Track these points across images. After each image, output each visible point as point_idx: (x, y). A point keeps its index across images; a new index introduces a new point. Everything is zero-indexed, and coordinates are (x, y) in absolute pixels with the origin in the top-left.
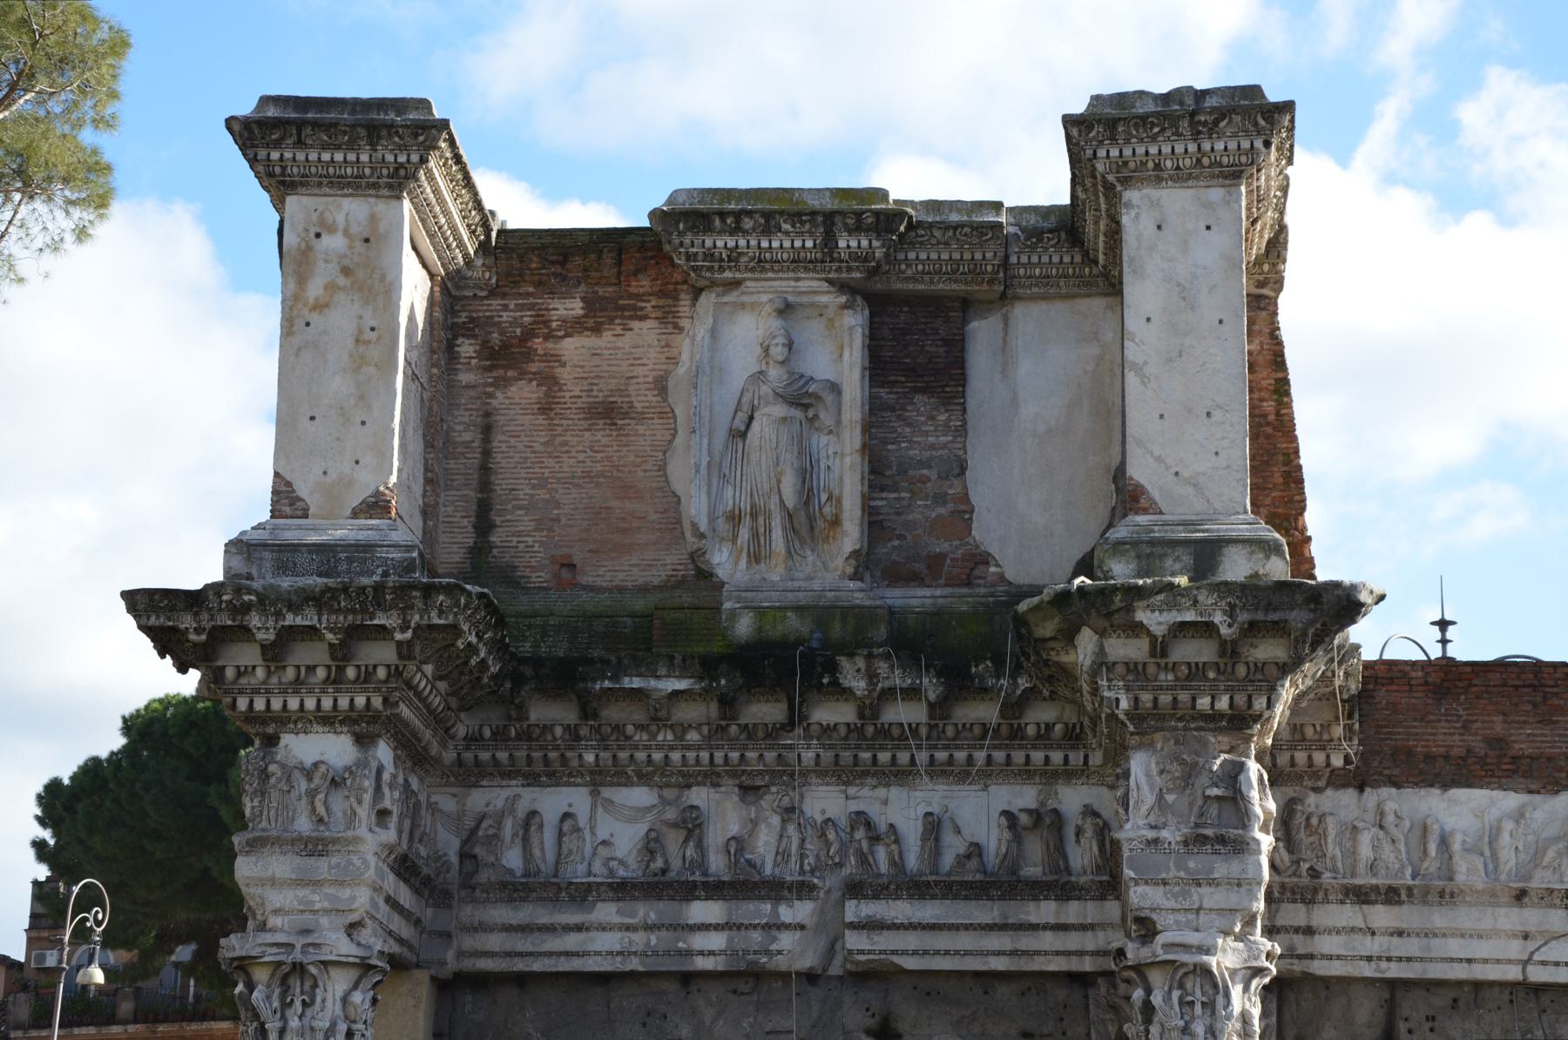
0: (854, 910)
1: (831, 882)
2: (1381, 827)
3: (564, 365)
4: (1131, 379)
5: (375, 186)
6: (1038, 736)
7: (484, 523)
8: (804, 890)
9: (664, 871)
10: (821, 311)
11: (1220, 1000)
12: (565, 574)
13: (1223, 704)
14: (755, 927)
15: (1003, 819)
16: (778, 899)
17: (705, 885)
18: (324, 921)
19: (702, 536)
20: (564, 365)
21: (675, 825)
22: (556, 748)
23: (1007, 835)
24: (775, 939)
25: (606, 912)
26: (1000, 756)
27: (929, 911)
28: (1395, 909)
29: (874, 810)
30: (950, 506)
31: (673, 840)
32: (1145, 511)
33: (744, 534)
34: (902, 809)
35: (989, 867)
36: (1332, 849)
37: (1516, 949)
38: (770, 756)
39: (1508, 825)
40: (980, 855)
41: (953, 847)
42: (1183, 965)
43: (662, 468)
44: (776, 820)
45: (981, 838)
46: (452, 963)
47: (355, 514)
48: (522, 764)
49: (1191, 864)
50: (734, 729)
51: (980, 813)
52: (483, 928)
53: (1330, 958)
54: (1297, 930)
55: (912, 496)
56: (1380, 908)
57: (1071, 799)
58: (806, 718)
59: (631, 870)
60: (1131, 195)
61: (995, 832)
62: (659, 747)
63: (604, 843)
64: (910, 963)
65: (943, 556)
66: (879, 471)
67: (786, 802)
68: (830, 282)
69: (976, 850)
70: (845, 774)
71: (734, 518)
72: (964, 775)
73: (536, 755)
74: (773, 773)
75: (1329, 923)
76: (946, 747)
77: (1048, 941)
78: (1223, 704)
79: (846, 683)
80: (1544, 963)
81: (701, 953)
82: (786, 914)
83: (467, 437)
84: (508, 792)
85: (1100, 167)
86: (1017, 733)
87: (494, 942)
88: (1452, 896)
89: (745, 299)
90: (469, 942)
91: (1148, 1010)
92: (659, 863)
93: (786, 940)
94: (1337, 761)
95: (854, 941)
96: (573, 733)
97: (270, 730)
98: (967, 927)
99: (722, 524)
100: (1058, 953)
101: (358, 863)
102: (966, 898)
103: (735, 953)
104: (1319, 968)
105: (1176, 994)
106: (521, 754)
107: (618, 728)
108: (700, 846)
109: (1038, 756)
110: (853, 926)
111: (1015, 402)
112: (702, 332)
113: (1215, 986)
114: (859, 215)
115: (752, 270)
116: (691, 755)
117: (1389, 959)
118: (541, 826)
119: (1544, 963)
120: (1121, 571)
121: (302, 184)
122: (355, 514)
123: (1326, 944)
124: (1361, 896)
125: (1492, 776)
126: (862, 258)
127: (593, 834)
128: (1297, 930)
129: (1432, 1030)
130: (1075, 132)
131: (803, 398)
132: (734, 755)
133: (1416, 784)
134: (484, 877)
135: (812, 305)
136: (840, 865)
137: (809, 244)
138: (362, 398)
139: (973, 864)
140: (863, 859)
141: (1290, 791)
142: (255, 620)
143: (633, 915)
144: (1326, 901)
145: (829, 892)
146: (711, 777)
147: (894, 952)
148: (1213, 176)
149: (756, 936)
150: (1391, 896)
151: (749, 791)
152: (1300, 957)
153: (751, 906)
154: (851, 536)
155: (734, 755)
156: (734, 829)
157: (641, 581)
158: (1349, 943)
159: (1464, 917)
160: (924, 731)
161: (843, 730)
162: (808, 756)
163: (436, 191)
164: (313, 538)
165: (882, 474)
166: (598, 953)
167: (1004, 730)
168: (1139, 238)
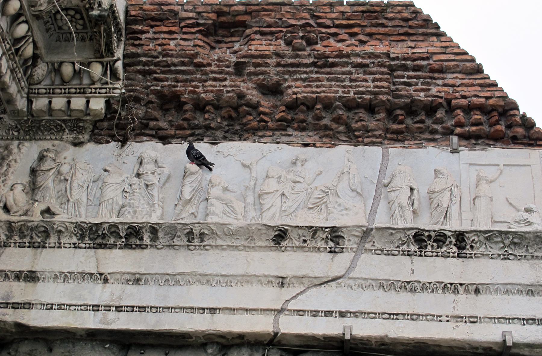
2: (138, 175)
53: (50, 307)
54: (18, 276)
56: (117, 252)
75: (57, 268)
80: (300, 313)
88: (202, 236)
94: (98, 105)
104: (36, 319)
117: (119, 309)
119: (300, 313)
123: (46, 292)
124: (96, 236)
125: (266, 128)
128: (18, 276)
141: (47, 144)
150: (132, 236)
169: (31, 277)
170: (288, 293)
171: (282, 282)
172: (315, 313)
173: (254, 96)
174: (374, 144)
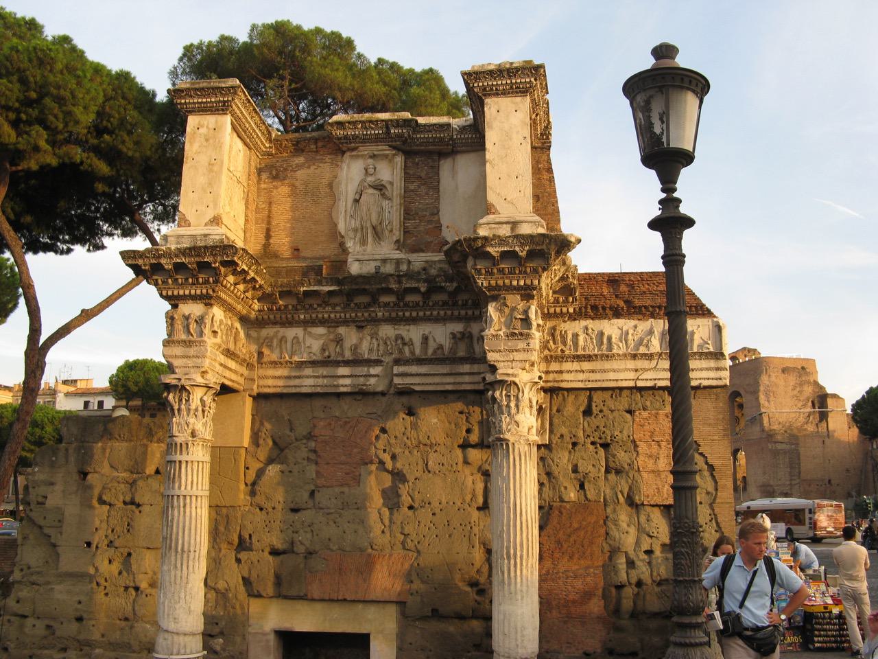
0: (396, 370)
1: (387, 359)
3: (297, 180)
4: (488, 165)
5: (218, 110)
6: (463, 305)
7: (268, 236)
8: (377, 362)
9: (329, 357)
10: (386, 156)
11: (521, 394)
12: (296, 253)
13: (522, 283)
14: (361, 376)
15: (451, 336)
16: (370, 366)
17: (343, 361)
18: (192, 370)
19: (343, 237)
20: (297, 180)
21: (332, 341)
22: (290, 313)
23: (452, 341)
24: (368, 380)
25: (308, 371)
26: (449, 312)
27: (423, 369)
28: (591, 363)
29: (404, 334)
30: (434, 225)
31: (332, 347)
32: (494, 213)
33: (359, 235)
34: (414, 333)
35: (446, 353)
36: (569, 342)
37: (632, 375)
38: (366, 314)
39: (631, 332)
40: (442, 348)
41: (432, 346)
42: (507, 381)
43: (330, 214)
44: (369, 338)
45: (443, 342)
46: (255, 391)
47: (206, 225)
48: (278, 319)
49: (510, 344)
50: (352, 305)
51: (441, 334)
52: (266, 377)
54: (557, 372)
55: (419, 222)
57: (475, 328)
58: (378, 300)
59: (318, 357)
60: (488, 101)
61: (448, 340)
62: (327, 312)
63: (308, 347)
64: (417, 388)
65: (432, 242)
66: (408, 214)
67: (373, 331)
68: (390, 146)
69: (441, 347)
70: (393, 321)
71: (356, 230)
72: (437, 320)
73: (283, 316)
74: (367, 321)
76: (430, 310)
77: (467, 379)
78: (522, 283)
79: (391, 287)
81: (342, 386)
82: (373, 371)
83: (263, 206)
84: (275, 330)
85: (475, 90)
86: (455, 304)
87: (270, 382)
89: (359, 153)
90: (262, 382)
91: (494, 399)
92: (327, 354)
93: (372, 381)
94: (571, 310)
95: (397, 380)
96: (295, 308)
97: (173, 302)
98: (437, 375)
99: (351, 234)
100: (470, 383)
101: (203, 349)
102: (437, 364)
103: (354, 385)
104: (564, 385)
105: (504, 392)
106: (278, 316)
107: (311, 306)
108: (341, 347)
109: (463, 312)
110: (397, 375)
111: (457, 188)
112: (345, 166)
113: (519, 389)
114: (397, 121)
115: (362, 143)
116: (338, 315)
118: (286, 342)
120: (482, 232)
121: (193, 111)
122: (206, 225)
123: (566, 376)
124: (579, 358)
126: (400, 136)
127: (305, 344)
130: (466, 77)
131: (380, 188)
132: (353, 315)
133: (599, 319)
134: (265, 359)
135: (384, 155)
136: (392, 354)
137: (381, 132)
138: (210, 184)
139: (439, 352)
140: (401, 351)
142: (163, 261)
143: (318, 372)
144: (567, 361)
145: (387, 363)
146: (345, 322)
147: (411, 384)
148: (517, 92)
149: (362, 379)
150: (589, 358)
151: (360, 328)
152: (556, 381)
153: (360, 369)
154: (397, 234)
155: (353, 315)
156: (354, 341)
157: (322, 254)
158: (574, 376)
159: (615, 364)
160: (421, 304)
161: (392, 305)
162: (380, 314)
163: (242, 113)
164: (189, 233)
165: (408, 214)
166: (306, 386)
167: (450, 302)
168: (491, 115)
169: (561, 372)
170: (638, 374)
171: (636, 370)
172: (647, 380)
173: (622, 304)
174: (660, 319)
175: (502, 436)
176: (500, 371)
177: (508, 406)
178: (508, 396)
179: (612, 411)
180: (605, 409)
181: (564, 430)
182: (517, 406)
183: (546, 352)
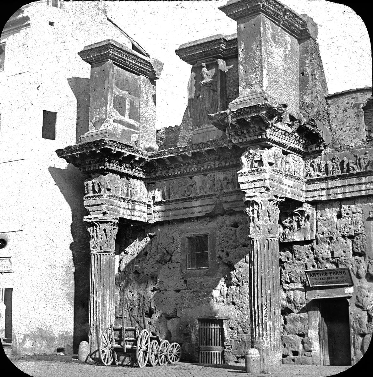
36: (323, 169)
129: (349, 210)
175: (249, 236)
176: (246, 195)
177: (253, 217)
178: (253, 211)
179: (353, 213)
180: (350, 212)
181: (325, 229)
182: (258, 217)
183: (309, 178)
